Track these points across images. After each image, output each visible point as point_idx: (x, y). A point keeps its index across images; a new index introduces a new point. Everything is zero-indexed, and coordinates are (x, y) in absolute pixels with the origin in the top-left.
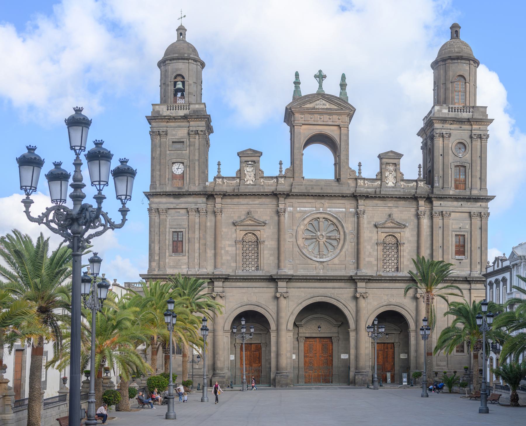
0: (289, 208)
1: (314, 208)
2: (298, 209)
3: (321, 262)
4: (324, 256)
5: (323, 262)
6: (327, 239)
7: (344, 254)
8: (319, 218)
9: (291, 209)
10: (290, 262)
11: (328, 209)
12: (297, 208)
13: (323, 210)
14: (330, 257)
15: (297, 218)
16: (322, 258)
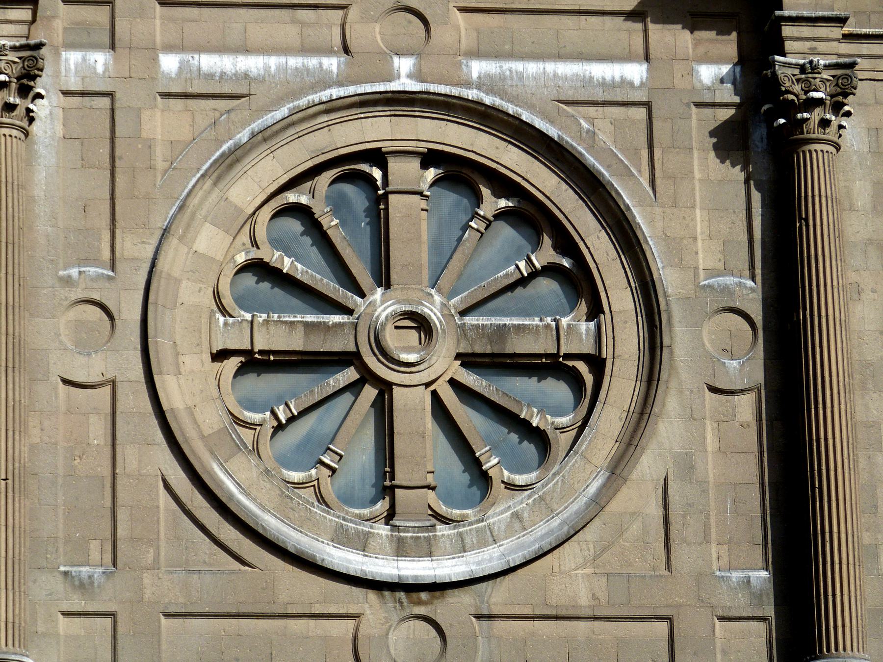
0: (73, 57)
1: (328, 52)
2: (169, 63)
3: (411, 588)
4: (442, 530)
5: (438, 588)
6: (468, 360)
7: (655, 510)
8: (378, 157)
9: (100, 60)
10: (84, 586)
11: (477, 68)
12: (152, 52)
13: (417, 75)
14: (507, 544)
15: (160, 153)
16: (427, 550)
